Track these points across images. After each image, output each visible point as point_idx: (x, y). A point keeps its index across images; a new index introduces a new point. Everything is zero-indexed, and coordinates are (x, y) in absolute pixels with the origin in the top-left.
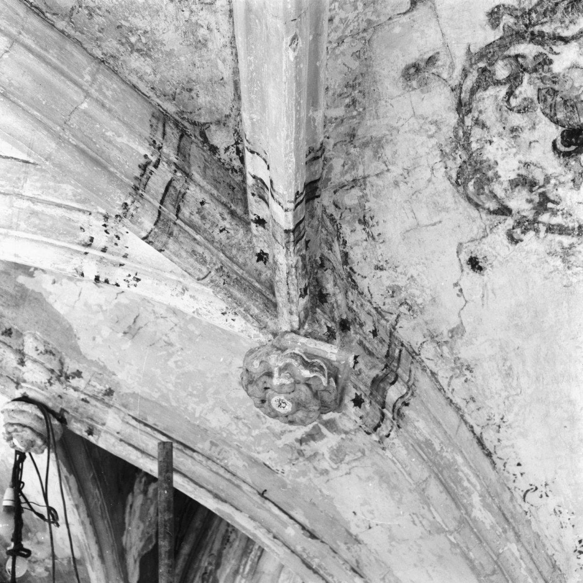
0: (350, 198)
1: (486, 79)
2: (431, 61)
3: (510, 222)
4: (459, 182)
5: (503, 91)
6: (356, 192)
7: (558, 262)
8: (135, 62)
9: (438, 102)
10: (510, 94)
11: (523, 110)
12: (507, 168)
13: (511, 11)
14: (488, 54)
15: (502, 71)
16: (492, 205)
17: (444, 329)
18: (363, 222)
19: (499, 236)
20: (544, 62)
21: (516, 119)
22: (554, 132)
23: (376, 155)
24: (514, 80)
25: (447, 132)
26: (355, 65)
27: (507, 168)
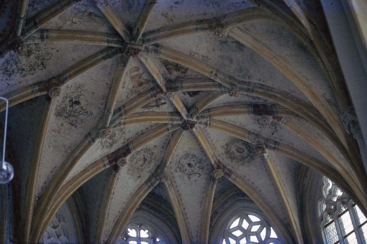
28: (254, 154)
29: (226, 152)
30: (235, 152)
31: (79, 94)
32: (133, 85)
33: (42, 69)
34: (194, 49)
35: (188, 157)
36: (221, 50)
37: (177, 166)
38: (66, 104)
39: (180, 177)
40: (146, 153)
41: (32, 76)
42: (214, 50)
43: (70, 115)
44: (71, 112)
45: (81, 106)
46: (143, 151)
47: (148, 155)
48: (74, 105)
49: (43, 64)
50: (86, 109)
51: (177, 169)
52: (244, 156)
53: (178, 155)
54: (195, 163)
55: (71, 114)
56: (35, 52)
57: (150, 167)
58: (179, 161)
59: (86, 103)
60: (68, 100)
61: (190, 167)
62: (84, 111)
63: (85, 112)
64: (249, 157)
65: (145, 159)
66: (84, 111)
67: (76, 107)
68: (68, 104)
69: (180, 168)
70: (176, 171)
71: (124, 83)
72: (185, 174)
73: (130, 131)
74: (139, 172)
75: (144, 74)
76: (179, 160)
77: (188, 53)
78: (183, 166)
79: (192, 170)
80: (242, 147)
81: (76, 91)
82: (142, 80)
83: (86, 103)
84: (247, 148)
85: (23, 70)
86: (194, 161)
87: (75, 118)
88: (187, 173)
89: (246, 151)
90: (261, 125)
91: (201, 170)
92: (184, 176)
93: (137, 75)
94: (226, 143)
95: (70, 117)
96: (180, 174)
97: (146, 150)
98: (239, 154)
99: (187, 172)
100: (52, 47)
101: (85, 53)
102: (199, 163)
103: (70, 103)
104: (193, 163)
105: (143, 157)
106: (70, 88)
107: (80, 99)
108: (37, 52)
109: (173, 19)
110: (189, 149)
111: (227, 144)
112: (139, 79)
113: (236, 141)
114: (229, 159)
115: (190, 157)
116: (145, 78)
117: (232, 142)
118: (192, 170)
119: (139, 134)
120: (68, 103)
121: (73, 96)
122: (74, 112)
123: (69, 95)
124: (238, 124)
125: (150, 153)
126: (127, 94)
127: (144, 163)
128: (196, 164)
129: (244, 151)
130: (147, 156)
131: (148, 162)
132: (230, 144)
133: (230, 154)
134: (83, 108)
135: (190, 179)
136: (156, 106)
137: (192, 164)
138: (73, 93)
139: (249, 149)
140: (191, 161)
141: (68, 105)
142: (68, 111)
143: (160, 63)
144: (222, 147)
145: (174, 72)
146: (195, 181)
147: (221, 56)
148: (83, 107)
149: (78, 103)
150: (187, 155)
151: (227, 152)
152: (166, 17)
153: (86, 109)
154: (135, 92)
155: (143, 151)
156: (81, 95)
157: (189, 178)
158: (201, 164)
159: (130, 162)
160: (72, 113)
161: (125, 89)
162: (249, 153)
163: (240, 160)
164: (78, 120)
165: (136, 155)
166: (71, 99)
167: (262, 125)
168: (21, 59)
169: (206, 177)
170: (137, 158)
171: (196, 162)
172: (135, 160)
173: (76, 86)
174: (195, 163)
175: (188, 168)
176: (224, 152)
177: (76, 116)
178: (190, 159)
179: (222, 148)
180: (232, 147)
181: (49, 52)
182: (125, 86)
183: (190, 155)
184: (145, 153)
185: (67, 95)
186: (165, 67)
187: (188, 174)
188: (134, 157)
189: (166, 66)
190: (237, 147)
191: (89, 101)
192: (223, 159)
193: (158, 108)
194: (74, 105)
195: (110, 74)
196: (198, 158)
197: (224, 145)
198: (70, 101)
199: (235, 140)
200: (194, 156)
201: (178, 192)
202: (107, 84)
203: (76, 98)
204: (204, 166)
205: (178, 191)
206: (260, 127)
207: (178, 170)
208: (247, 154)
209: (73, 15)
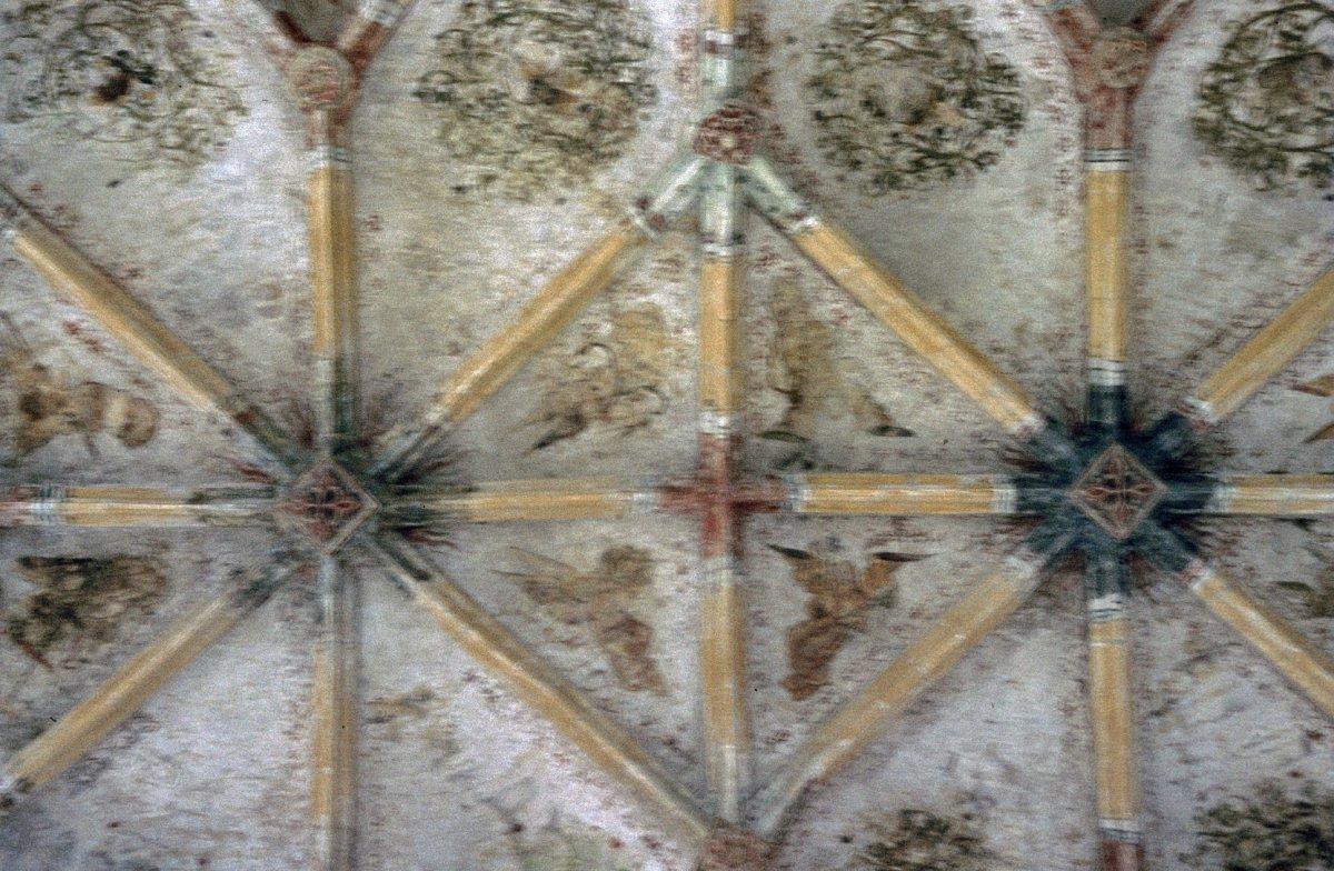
31: (151, 126)
33: (424, 80)
34: (158, 741)
36: (102, 854)
41: (438, 30)
42: (114, 825)
43: (82, 28)
48: (113, 71)
49: (441, 97)
56: (532, 111)
59: (85, 127)
60: (166, 66)
67: (96, 76)
71: (94, 346)
77: (151, 710)
82: (50, 423)
85: (499, 20)
93: (98, 414)
100: (497, 188)
101: (378, 283)
107: (122, 111)
108: (518, 119)
109: (384, 729)
116: (57, 442)
121: (161, 98)
122: (82, 53)
126: (19, 320)
138: (182, 107)
142: (115, 34)
143: (110, 548)
152: (405, 703)
168: (552, 46)
173: (207, 141)
181: (480, 157)
191: (88, 143)
194: (113, 71)
195: (185, 314)
202: (134, 273)
209: (624, 363)
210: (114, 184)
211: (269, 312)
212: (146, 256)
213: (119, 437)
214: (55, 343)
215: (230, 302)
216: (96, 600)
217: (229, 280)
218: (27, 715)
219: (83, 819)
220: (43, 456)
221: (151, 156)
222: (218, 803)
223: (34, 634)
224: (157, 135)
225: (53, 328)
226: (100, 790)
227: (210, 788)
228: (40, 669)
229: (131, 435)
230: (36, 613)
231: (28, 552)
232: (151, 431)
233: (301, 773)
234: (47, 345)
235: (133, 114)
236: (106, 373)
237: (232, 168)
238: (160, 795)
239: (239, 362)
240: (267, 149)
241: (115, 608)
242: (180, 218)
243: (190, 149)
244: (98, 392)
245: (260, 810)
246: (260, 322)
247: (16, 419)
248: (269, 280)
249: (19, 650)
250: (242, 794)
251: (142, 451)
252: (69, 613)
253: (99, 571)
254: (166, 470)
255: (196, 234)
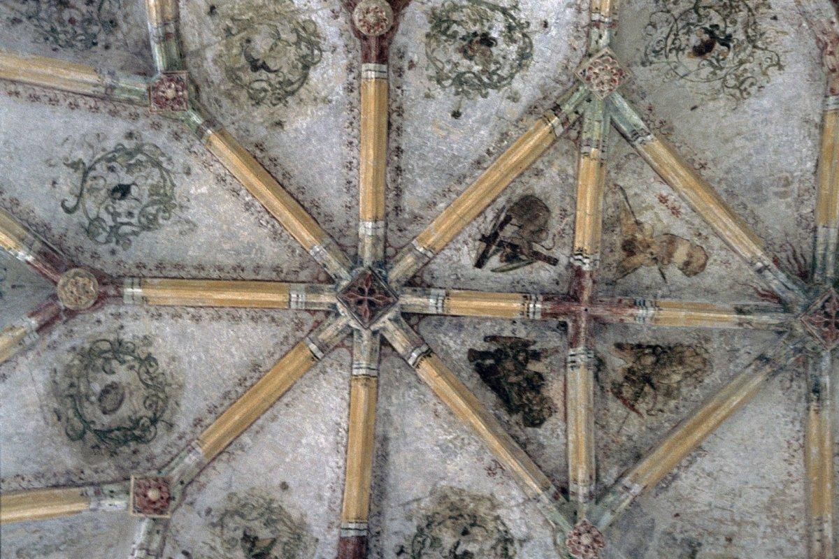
0: (564, 78)
1: (501, 79)
2: (509, 98)
3: (525, 30)
4: (529, 56)
5: (499, 72)
6: (561, 78)
7: (520, 6)
8: (571, 172)
9: (517, 84)
10: (498, 69)
11: (497, 62)
12: (514, 48)
13: (481, 93)
14: (495, 87)
15: (495, 77)
16: (527, 40)
17: (573, 10)
18: (567, 68)
19: (532, 27)
20: (483, 71)
21: (501, 60)
22: (493, 49)
23: (545, 84)
24: (494, 73)
25: (522, 73)
26: (525, 118)
27: (514, 48)
28: (93, 447)
29: (120, 343)
30: (110, 379)
31: (720, 73)
32: (646, 226)
35: (153, 203)
36: (670, 534)
37: (146, 147)
38: (734, 22)
39: (98, 135)
40: (280, 83)
42: (677, 515)
43: (696, 9)
44: (699, 15)
45: (686, 52)
46: (295, 77)
47: (264, 85)
48: (706, 37)
50: (667, 57)
51: (135, 141)
52: (86, 404)
53: (188, 173)
54: (119, 215)
55: (697, 12)
57: (215, 62)
58: (158, 164)
59: (681, 71)
61: (115, 190)
62: (668, 48)
63: (662, 49)
64: (79, 425)
65: (256, 66)
66: (668, 48)
67: (694, 40)
68: (726, 26)
69: (130, 154)
70: (130, 135)
71: (675, 211)
72: (98, 156)
73: (428, 96)
74: (233, 19)
75: (659, 276)
76: (164, 165)
78: (129, 169)
79: (99, 190)
80: (125, 411)
81: (739, 72)
83: (681, 71)
84: (118, 429)
86: (130, 214)
87: (676, 13)
88: (98, 166)
89: (106, 420)
90: (221, 519)
91: (87, 222)
92: (91, 152)
93: (670, 255)
94: (155, 360)
95: (692, 6)
96: (110, 145)
97: (289, 89)
98: (97, 388)
99: (101, 168)
102: (115, 229)
103: (724, 32)
104: (123, 206)
105: (272, 64)
106: (764, 66)
107: (705, 62)
110: (188, 222)
111: (149, 360)
112: (652, 254)
113: (154, 399)
114: (87, 346)
115: (152, 210)
116: (641, 271)
117: (150, 382)
118: (99, 190)
119: (394, 116)
120: (729, 31)
121: (731, 55)
122: (693, 24)
123: (750, 48)
124: (246, 439)
125: (263, 94)
126: (630, 192)
127: (248, 57)
128: (115, 215)
129: (105, 413)
130: (261, 80)
131: (239, 69)
132: (148, 372)
133: (109, 355)
134: (674, 52)
135: (68, 165)
136: (495, 235)
137: (122, 202)
138: (741, 63)
139: (113, 435)
140: (133, 203)
141: (722, 25)
142: (712, 12)
143: (672, 340)
144: (147, 340)
145: (622, 362)
146: (54, 183)
147: (653, 528)
148: (677, 55)
149: (702, 50)
150: (164, 200)
151: (118, 349)
153: (667, 57)
154: (619, 220)
155: (295, 77)
156: (714, 74)
157: (75, 165)
158: (105, 234)
159: (300, 21)
160: (695, 15)
161: (651, 199)
162: (96, 431)
163: (72, 385)
164: (665, 16)
165: (304, 50)
166: (732, 45)
167: (221, 524)
169: (54, 231)
170: (293, 49)
171: (119, 220)
172: (293, 38)
173: (752, 84)
174: (119, 215)
175: (113, 180)
176: (122, 336)
177: (676, 20)
178: (144, 203)
179: (145, 337)
180: (133, 374)
182: (663, 207)
183: (158, 211)
184: (281, 79)
185: (755, 47)
186: (653, 344)
187: (92, 168)
188: (303, 45)
189: (654, 348)
190: (127, 391)
191: (682, 81)
192: (99, 321)
193: (479, 236)
194: (706, 37)
196: (134, 233)
197: (151, 350)
198: (729, 38)
199: (161, 395)
200: (150, 224)
201: (50, 100)
202: (703, 166)
203: (721, 57)
204: (98, 243)
205: (53, 102)
206: (209, 511)
207: (129, 145)
208: (93, 422)
210: (694, 108)
211: (783, 195)
212: (709, 155)
213: (681, 269)
214: (652, 208)
215: (758, 187)
216: (665, 372)
217: (757, 173)
218: (629, 445)
219: (661, 513)
220: (632, 279)
221: (718, 92)
222: (739, 503)
223: (628, 392)
224: (724, 80)
225: (651, 199)
226: (671, 493)
227: (735, 494)
228: (633, 414)
229: (688, 268)
230: (626, 378)
231: (620, 339)
232: (703, 266)
233: (797, 485)
234: (646, 209)
235: (711, 64)
236: (679, 228)
237: (766, 103)
238: (704, 497)
239: (760, 225)
240: (790, 93)
241: (676, 378)
242: (729, 133)
243: (742, 88)
244: (672, 240)
245: (768, 509)
246: (774, 201)
247: (619, 254)
248: (785, 174)
249: (619, 402)
250: (753, 498)
251: (695, 279)
252: (647, 380)
253: (665, 354)
254: (708, 291)
255: (739, 142)
